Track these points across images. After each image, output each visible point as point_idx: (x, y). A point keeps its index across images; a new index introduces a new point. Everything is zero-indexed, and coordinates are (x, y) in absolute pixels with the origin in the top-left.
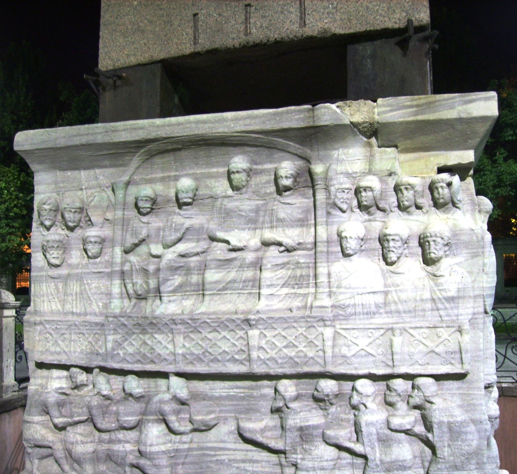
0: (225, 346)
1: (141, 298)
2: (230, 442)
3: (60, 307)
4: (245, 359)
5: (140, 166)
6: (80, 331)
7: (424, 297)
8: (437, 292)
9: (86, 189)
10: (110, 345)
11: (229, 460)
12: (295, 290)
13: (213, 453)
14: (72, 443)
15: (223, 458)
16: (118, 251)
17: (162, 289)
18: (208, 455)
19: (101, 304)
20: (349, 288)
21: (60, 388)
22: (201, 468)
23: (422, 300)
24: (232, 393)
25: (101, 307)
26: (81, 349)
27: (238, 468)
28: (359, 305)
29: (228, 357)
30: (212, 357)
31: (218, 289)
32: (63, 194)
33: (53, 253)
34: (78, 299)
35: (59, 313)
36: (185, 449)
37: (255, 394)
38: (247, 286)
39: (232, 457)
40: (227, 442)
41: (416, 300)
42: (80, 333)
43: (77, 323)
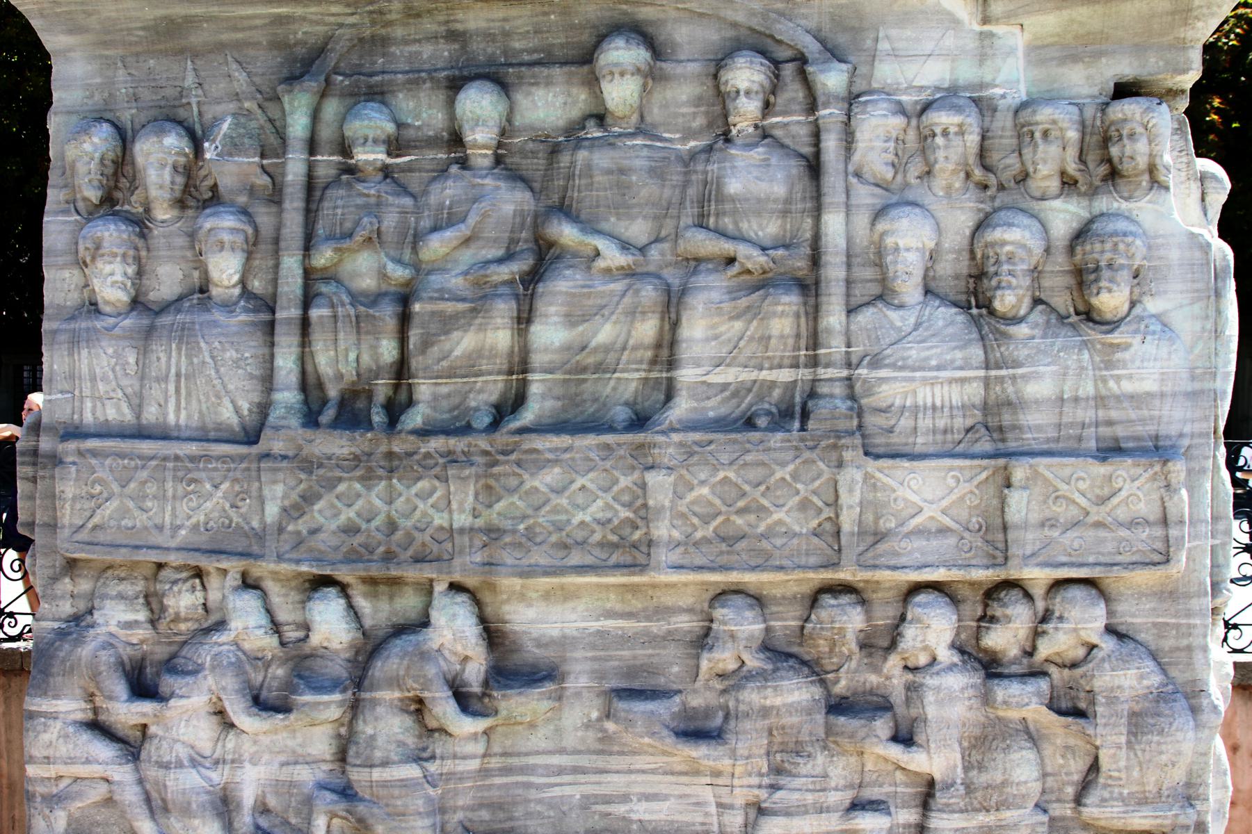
7: (1081, 393)
8: (1112, 384)
10: (272, 511)
12: (764, 372)
14: (166, 766)
15: (567, 791)
17: (416, 363)
20: (902, 368)
22: (511, 819)
23: (1076, 399)
25: (246, 413)
26: (194, 520)
28: (925, 408)
33: (112, 274)
34: (183, 391)
36: (468, 772)
41: (1062, 400)
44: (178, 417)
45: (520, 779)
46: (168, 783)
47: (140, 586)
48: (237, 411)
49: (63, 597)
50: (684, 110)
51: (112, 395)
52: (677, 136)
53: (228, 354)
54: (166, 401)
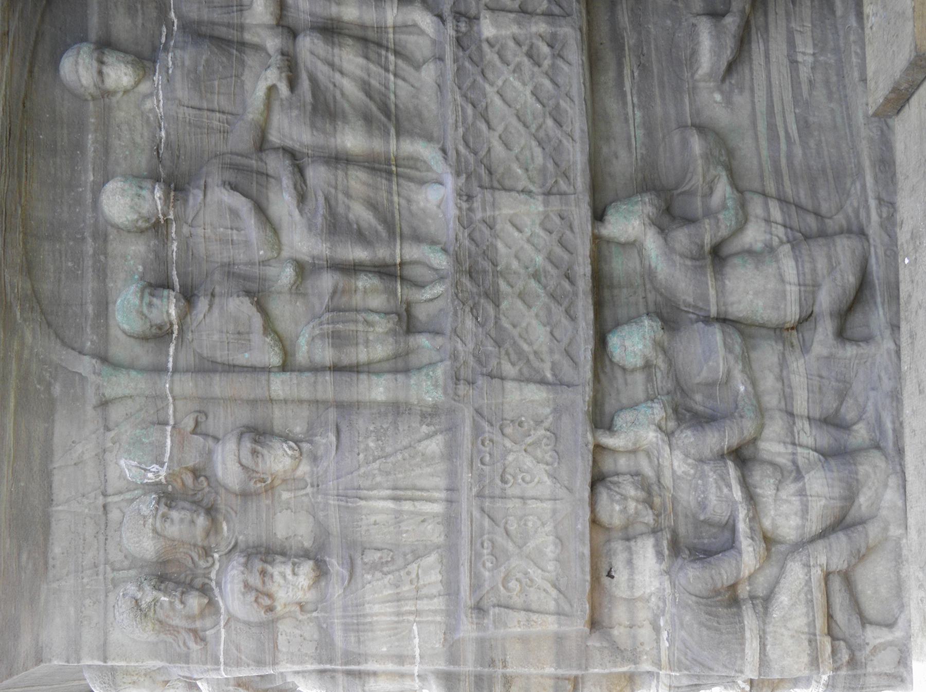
0: (521, 92)
1: (407, 322)
2: (753, 103)
3: (432, 558)
4: (551, 46)
5: (57, 336)
6: (498, 481)
9: (105, 495)
11: (796, 102)
13: (783, 146)
16: (279, 385)
18: (790, 157)
19: (424, 429)
21: (659, 554)
24: (635, 100)
26: (545, 478)
27: (811, 83)
29: (547, 83)
30: (550, 122)
31: (383, 118)
32: (113, 570)
35: (451, 568)
37: (632, 42)
38: (380, 55)
39: (788, 96)
40: (754, 109)
42: (504, 481)
43: (475, 490)
44: (436, 489)
45: (783, 161)
46: (823, 502)
47: (618, 546)
48: (428, 436)
49: (634, 637)
50: (140, 21)
51: (414, 576)
52: (164, 29)
53: (372, 444)
54: (420, 514)
